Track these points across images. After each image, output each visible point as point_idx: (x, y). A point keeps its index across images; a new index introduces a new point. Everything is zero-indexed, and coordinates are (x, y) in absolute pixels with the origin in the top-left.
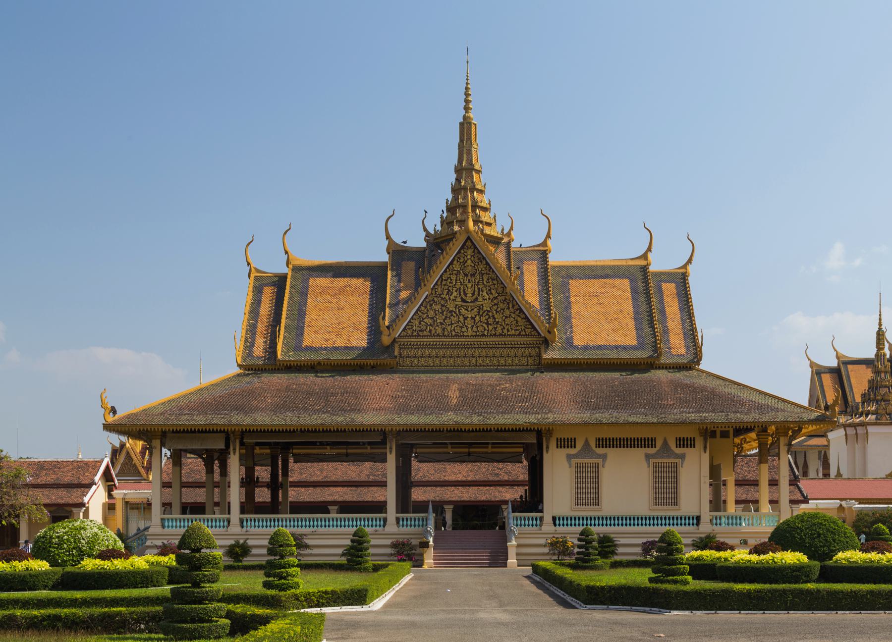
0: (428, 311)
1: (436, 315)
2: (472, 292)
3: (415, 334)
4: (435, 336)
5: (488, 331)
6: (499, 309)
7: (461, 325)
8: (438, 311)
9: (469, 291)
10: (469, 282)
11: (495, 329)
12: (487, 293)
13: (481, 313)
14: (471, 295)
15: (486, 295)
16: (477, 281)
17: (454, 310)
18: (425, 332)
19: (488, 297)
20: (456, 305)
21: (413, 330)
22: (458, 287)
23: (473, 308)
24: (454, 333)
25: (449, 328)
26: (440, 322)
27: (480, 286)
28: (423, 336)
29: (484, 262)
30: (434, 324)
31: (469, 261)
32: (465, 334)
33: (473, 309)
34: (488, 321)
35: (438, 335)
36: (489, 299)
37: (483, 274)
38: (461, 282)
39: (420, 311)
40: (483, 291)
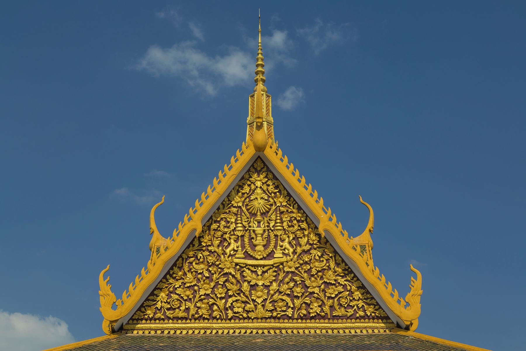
0: (185, 274)
1: (199, 280)
2: (265, 243)
3: (159, 315)
4: (195, 319)
7: (245, 299)
9: (259, 241)
10: (259, 226)
11: (308, 305)
12: (290, 243)
13: (280, 278)
15: (288, 246)
17: (233, 273)
18: (177, 310)
19: (291, 250)
20: (237, 264)
21: (157, 308)
23: (266, 269)
24: (230, 314)
26: (205, 295)
27: (279, 233)
28: (174, 318)
31: (259, 191)
33: (267, 271)
36: (294, 253)
37: (282, 213)
38: (244, 227)
39: (171, 276)
40: (283, 241)
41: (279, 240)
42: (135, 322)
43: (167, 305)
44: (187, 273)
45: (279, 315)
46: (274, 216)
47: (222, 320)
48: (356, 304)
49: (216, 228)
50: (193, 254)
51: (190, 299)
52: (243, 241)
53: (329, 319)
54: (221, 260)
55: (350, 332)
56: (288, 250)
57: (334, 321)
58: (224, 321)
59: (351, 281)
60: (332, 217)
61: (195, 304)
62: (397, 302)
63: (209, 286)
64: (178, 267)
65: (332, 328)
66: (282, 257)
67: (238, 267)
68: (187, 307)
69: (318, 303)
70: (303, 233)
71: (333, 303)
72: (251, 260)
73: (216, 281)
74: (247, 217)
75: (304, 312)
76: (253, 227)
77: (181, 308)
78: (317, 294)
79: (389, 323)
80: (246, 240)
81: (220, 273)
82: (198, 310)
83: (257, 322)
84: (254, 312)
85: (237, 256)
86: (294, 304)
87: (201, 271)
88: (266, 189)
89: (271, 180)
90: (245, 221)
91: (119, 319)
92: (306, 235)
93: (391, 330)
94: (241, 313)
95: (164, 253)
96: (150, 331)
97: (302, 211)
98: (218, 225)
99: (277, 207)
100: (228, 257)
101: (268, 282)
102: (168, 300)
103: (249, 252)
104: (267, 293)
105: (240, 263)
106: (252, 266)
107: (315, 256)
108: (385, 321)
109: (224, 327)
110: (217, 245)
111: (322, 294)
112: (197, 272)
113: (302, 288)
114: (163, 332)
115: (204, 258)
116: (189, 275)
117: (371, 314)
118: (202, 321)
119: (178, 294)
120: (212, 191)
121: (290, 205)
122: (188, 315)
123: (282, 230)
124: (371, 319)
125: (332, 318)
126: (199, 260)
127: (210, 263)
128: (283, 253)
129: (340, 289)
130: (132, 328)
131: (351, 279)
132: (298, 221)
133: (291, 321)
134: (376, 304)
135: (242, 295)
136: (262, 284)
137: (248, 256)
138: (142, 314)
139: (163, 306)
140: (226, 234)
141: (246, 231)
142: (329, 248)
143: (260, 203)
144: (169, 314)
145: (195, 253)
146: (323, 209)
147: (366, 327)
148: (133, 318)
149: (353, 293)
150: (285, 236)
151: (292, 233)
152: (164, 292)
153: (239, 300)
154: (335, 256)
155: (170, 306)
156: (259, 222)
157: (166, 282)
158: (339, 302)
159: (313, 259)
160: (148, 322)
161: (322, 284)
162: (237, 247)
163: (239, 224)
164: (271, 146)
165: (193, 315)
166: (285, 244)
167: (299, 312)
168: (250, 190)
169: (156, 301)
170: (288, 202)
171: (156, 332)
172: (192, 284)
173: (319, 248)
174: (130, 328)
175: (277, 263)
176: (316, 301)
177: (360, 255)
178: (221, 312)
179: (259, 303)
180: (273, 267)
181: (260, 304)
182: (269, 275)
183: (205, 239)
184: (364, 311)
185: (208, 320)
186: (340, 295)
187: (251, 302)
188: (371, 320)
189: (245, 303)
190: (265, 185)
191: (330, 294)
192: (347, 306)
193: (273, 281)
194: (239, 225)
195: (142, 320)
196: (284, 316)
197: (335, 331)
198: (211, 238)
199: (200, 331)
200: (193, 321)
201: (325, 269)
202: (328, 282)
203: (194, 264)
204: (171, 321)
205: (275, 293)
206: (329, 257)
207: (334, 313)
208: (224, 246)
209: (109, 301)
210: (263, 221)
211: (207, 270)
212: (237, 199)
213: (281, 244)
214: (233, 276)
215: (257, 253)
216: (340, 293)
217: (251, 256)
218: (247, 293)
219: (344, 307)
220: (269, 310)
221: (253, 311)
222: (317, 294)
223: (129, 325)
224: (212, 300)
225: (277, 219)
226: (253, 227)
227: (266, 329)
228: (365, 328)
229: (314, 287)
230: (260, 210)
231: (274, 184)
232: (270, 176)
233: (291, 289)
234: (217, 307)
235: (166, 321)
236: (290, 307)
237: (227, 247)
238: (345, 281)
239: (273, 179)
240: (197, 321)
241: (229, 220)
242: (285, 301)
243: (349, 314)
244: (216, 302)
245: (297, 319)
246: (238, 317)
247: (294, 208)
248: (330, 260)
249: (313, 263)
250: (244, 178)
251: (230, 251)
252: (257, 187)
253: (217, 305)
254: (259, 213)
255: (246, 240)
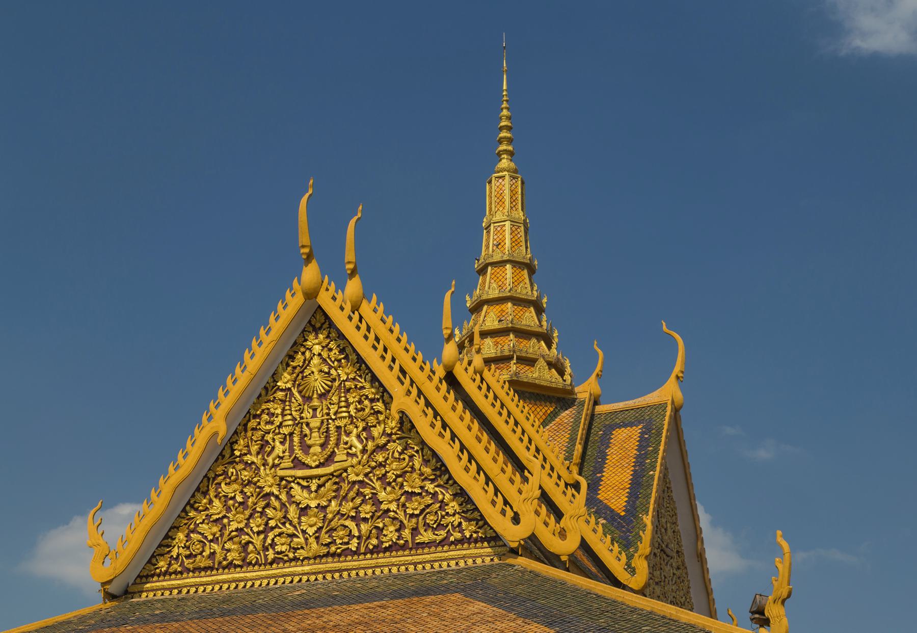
0: (211, 502)
1: (228, 510)
2: (322, 441)
3: (176, 567)
4: (224, 568)
5: (359, 538)
6: (391, 476)
8: (233, 498)
9: (315, 439)
10: (314, 416)
11: (380, 530)
12: (358, 437)
13: (342, 493)
14: (318, 449)
16: (334, 408)
17: (276, 493)
18: (199, 557)
19: (360, 447)
20: (282, 479)
22: (285, 431)
23: (323, 479)
24: (271, 555)
25: (258, 541)
26: (237, 530)
27: (341, 423)
29: (353, 357)
30: (222, 535)
31: (316, 360)
32: (301, 553)
33: (323, 485)
34: (358, 512)
35: (231, 565)
36: (364, 451)
37: (348, 390)
38: (294, 419)
39: (192, 506)
40: (348, 434)
41: (343, 433)
42: (144, 580)
43: (185, 551)
44: (214, 499)
45: (339, 551)
46: (337, 398)
47: (260, 565)
48: (450, 522)
49: (254, 427)
50: (223, 470)
51: (217, 538)
52: (292, 441)
53: (411, 549)
54: (260, 475)
55: (449, 566)
56: (356, 448)
57: (418, 552)
58: (263, 567)
59: (445, 485)
60: (410, 388)
61: (224, 546)
62: (501, 513)
63: (243, 516)
64: (203, 493)
65: (415, 562)
66: (346, 459)
67: (284, 482)
68: (212, 551)
69: (394, 525)
70: (378, 419)
71: (417, 523)
72: (303, 469)
73: (252, 507)
74: (299, 403)
75: (374, 541)
76: (307, 418)
77: (204, 554)
78: (393, 511)
79: (499, 546)
80: (296, 439)
81: (259, 494)
82: (227, 553)
83: (309, 565)
84: (304, 550)
85: (282, 466)
86: (359, 531)
87: (233, 495)
88: (327, 356)
89: (335, 340)
90: (296, 411)
91: (113, 579)
92: (381, 421)
93: (500, 558)
94: (286, 553)
95: (173, 475)
96: (162, 591)
97: (377, 383)
98: (258, 420)
99: (341, 383)
100: (271, 469)
101: (324, 501)
102: (187, 544)
103: (300, 458)
104: (322, 518)
105: (286, 477)
106: (303, 478)
107: (393, 452)
108: (493, 543)
109: (262, 576)
110: (255, 452)
111: (402, 510)
112: (227, 496)
113: (373, 505)
114: (180, 592)
115: (237, 475)
116: (216, 502)
117: (471, 536)
118: (232, 570)
119: (200, 533)
120: (243, 371)
121: (360, 376)
122: (214, 563)
123: (347, 418)
124: (473, 543)
125: (415, 546)
126: (230, 478)
127: (244, 481)
128: (348, 454)
129: (428, 500)
130: (139, 590)
131: (445, 483)
132: (372, 401)
133: (356, 557)
134: (479, 518)
135: (287, 525)
136: (316, 505)
137: (298, 464)
138: (152, 568)
139: (180, 552)
140: (269, 433)
141: (297, 424)
142: (414, 438)
143: (317, 379)
144: (188, 564)
145: (226, 467)
146: (399, 378)
147: (464, 557)
148: (141, 574)
149: (447, 505)
150: (351, 427)
151: (362, 420)
152: (183, 532)
153: (283, 533)
154: (422, 449)
155: (189, 553)
156: (315, 410)
157: (185, 516)
158: (425, 522)
159: (390, 457)
160: (162, 578)
161: (402, 495)
162: (284, 452)
163: (288, 416)
164: (327, 288)
165: (220, 563)
166: (351, 439)
167: (367, 543)
168: (305, 360)
169: (171, 546)
170: (358, 372)
171: (171, 592)
172: (220, 516)
173: (398, 439)
174: (136, 590)
175: (338, 470)
176: (392, 523)
177: (449, 443)
178: (259, 553)
179: (311, 534)
180: (333, 476)
181: (312, 536)
182: (326, 489)
183: (239, 445)
184: (462, 531)
185: (241, 567)
186: (428, 510)
187: (299, 534)
188: (473, 545)
189: (293, 536)
190: (326, 349)
191: (413, 509)
192: (437, 526)
193: (332, 498)
194: (289, 417)
195: (153, 576)
196: (346, 551)
197: (420, 567)
198: (248, 443)
199: (229, 586)
200: (221, 571)
201: (407, 472)
202: (410, 491)
203: (223, 485)
204: (191, 574)
205: (334, 516)
206: (413, 453)
207: (418, 539)
208: (266, 452)
209: (100, 553)
210: (321, 407)
211: (242, 492)
212: (286, 376)
213: (348, 439)
214: (277, 497)
215: (311, 458)
216: (428, 506)
217: (304, 463)
218: (295, 521)
219: (433, 527)
220: (324, 543)
221: (302, 548)
222: (393, 511)
223: (136, 585)
224: (247, 537)
225: (341, 402)
226: (307, 418)
227: (320, 573)
228: (464, 557)
229: (390, 502)
230: (317, 391)
231: (338, 346)
232: (334, 335)
233: (357, 508)
234: (253, 547)
235: (185, 575)
236: (354, 536)
237: (269, 455)
238: (436, 486)
239: (337, 339)
240: (226, 571)
241: (272, 410)
242: (347, 528)
243: (439, 538)
244: (251, 540)
245: (365, 554)
246: (282, 559)
247: (365, 381)
248: (416, 457)
249: (389, 465)
250: (297, 343)
251: (274, 460)
252: (314, 355)
253: (252, 543)
254: (315, 396)
255: (296, 439)
